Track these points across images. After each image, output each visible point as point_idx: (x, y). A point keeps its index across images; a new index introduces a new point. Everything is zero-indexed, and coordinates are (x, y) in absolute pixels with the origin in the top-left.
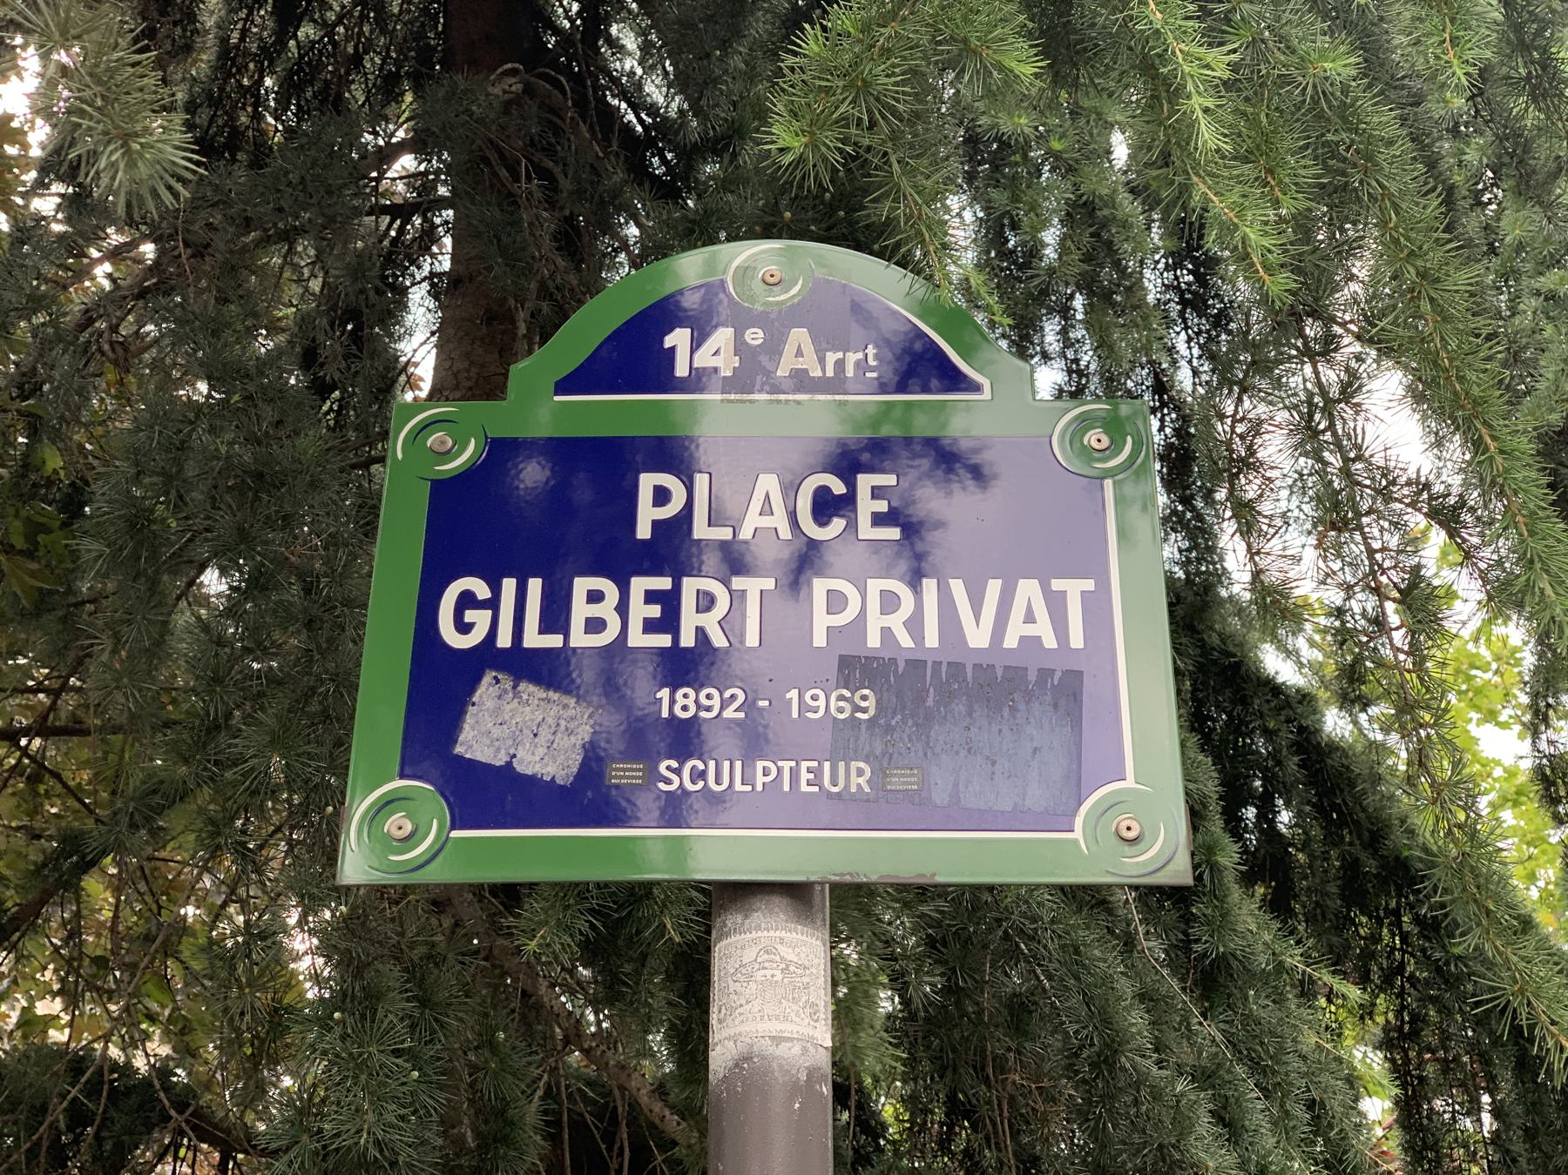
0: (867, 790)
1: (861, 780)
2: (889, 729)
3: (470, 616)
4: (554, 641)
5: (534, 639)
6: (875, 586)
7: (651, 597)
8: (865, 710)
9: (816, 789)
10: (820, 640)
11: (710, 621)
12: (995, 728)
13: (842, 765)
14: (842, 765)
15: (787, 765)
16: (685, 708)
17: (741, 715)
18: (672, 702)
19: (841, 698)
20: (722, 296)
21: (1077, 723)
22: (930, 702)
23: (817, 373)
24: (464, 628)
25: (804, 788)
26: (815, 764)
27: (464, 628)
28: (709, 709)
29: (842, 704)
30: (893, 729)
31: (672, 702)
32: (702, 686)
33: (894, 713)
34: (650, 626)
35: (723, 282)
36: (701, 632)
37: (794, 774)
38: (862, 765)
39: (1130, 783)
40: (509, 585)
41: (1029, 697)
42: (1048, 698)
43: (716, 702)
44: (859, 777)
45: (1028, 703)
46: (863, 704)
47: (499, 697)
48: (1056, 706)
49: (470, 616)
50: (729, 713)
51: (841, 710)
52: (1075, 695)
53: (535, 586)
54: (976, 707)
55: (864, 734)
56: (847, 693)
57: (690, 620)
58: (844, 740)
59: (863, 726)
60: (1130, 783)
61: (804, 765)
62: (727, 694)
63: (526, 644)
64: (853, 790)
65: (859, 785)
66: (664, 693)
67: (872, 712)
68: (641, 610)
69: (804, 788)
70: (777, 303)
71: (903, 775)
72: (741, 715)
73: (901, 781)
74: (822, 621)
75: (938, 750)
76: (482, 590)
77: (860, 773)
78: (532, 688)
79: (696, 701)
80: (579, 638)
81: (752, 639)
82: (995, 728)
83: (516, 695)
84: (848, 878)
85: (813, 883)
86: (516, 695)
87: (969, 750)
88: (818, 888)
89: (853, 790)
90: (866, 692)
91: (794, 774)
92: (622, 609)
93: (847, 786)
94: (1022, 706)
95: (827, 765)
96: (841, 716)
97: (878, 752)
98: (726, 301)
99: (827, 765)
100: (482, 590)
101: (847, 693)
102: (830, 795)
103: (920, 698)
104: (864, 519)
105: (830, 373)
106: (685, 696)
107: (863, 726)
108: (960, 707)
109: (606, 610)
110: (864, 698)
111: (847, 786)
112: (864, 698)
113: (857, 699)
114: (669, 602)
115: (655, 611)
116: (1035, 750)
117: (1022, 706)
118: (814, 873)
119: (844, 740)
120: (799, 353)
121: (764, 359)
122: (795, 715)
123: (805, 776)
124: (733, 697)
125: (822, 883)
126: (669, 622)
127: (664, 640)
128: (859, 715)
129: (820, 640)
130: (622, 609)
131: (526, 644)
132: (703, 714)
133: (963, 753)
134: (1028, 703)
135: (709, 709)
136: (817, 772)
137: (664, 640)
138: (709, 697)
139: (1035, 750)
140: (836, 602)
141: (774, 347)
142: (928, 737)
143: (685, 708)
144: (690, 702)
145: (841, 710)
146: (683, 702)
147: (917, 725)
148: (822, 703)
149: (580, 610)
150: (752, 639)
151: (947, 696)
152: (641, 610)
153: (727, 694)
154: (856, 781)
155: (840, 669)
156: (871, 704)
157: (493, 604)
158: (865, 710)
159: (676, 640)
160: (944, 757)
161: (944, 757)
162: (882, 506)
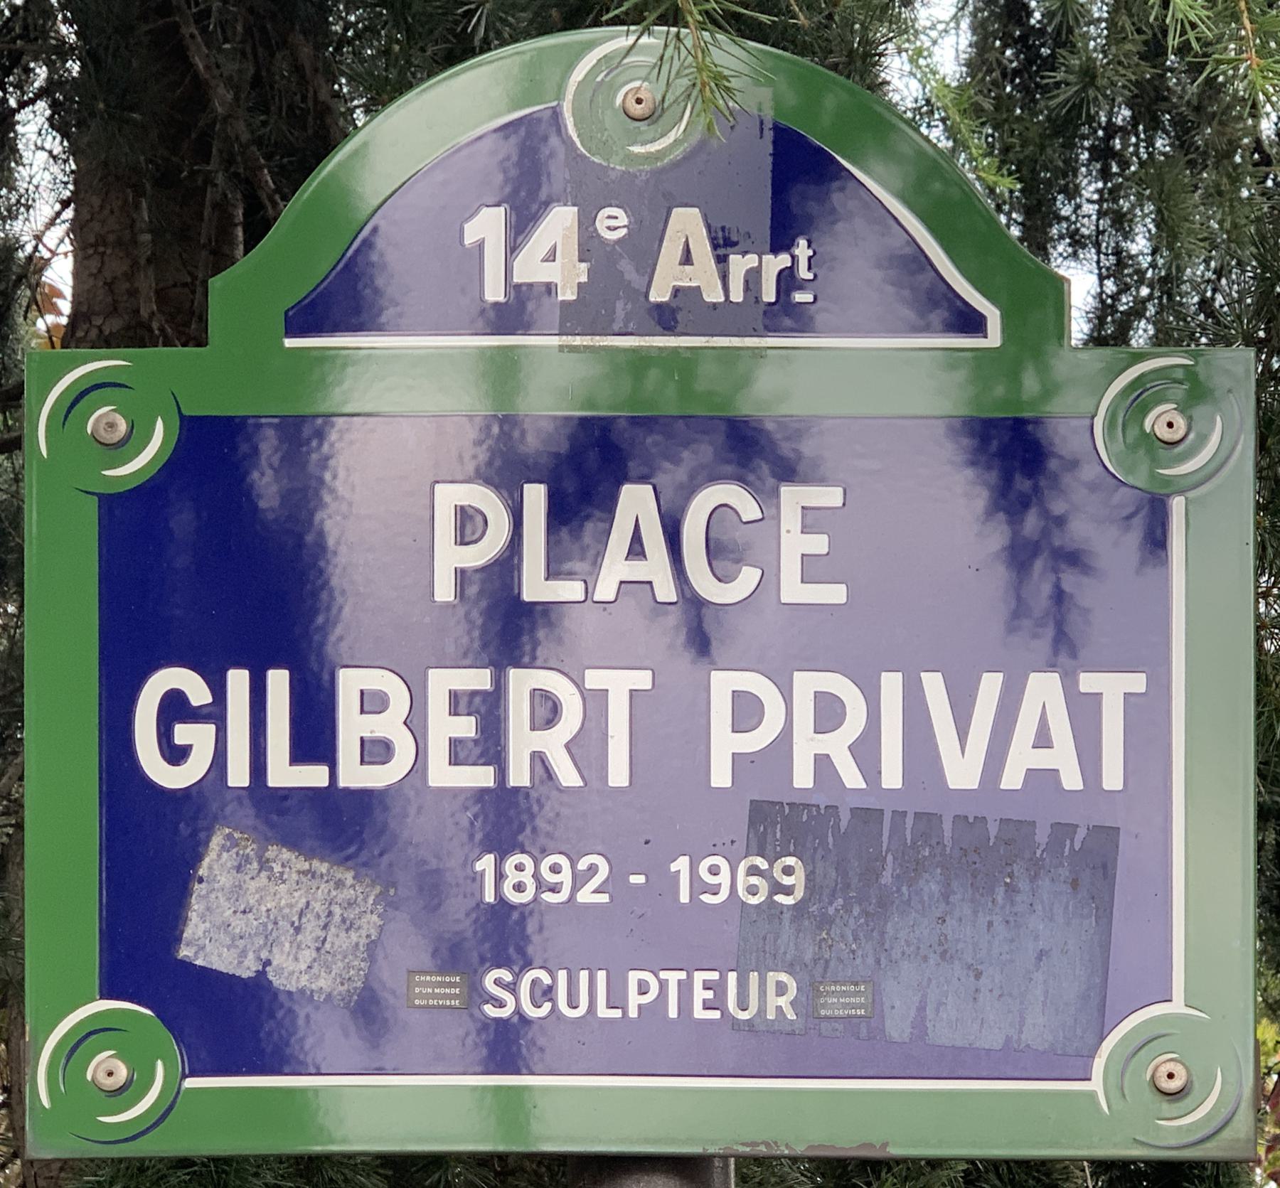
0: (791, 1015)
1: (783, 1001)
2: (825, 921)
3: (183, 733)
4: (314, 776)
5: (284, 773)
6: (807, 684)
7: (457, 703)
8: (788, 891)
9: (716, 1015)
10: (721, 776)
11: (554, 743)
12: (983, 920)
13: (754, 976)
14: (754, 976)
15: (673, 977)
16: (519, 887)
17: (604, 898)
18: (500, 876)
19: (754, 871)
20: (554, 141)
21: (1104, 912)
22: (887, 878)
23: (714, 295)
24: (175, 754)
25: (699, 1013)
26: (714, 976)
27: (175, 754)
28: (554, 889)
29: (754, 880)
30: (831, 921)
31: (500, 876)
32: (545, 852)
33: (833, 896)
34: (458, 753)
35: (556, 114)
36: (539, 760)
37: (685, 989)
38: (784, 977)
39: (1177, 1006)
40: (238, 681)
41: (1036, 869)
42: (1064, 872)
43: (566, 877)
44: (778, 996)
45: (1034, 879)
46: (787, 881)
47: (239, 868)
48: (1075, 884)
49: (183, 733)
50: (586, 896)
51: (753, 891)
52: (1104, 867)
53: (278, 681)
54: (955, 884)
55: (787, 929)
56: (762, 863)
57: (522, 741)
58: (753, 938)
59: (787, 916)
60: (1177, 1006)
61: (699, 977)
62: (583, 865)
63: (272, 782)
64: (771, 1015)
65: (779, 1009)
66: (486, 863)
67: (799, 893)
68: (447, 726)
69: (699, 1013)
70: (648, 157)
71: (845, 994)
72: (604, 898)
73: (841, 1002)
74: (725, 745)
75: (896, 954)
76: (198, 692)
77: (781, 989)
78: (286, 854)
79: (536, 876)
80: (354, 774)
81: (618, 775)
82: (983, 920)
83: (264, 864)
84: (763, 1150)
85: (713, 1156)
86: (264, 864)
87: (943, 955)
88: (717, 1163)
89: (771, 1015)
90: (790, 861)
91: (685, 989)
92: (416, 723)
93: (762, 1010)
94: (1024, 885)
95: (732, 977)
96: (754, 901)
97: (808, 956)
98: (561, 155)
99: (732, 977)
100: (198, 692)
101: (762, 863)
102: (735, 1023)
103: (871, 872)
104: (790, 569)
105: (737, 295)
106: (520, 868)
107: (787, 916)
108: (931, 886)
109: (390, 725)
110: (788, 871)
111: (762, 1010)
112: (788, 871)
113: (777, 873)
114: (489, 709)
115: (466, 727)
116: (1041, 955)
117: (1024, 885)
118: (713, 1142)
119: (753, 938)
120: (687, 259)
121: (627, 267)
122: (684, 897)
123: (700, 995)
124: (593, 869)
125: (725, 1158)
126: (489, 745)
127: (483, 777)
128: (780, 898)
129: (721, 776)
130: (416, 723)
131: (272, 782)
132: (548, 897)
133: (933, 959)
134: (1034, 879)
135: (554, 889)
136: (717, 988)
137: (483, 777)
138: (555, 869)
139: (1041, 955)
140: (746, 712)
141: (644, 244)
142: (882, 933)
143: (519, 887)
144: (527, 877)
145: (753, 891)
146: (515, 878)
147: (867, 914)
148: (724, 878)
149: (351, 727)
150: (618, 775)
151: (912, 869)
152: (447, 726)
153: (583, 865)
154: (774, 1001)
155: (752, 823)
156: (797, 880)
157: (216, 714)
158: (788, 891)
159: (502, 774)
160: (905, 965)
161: (905, 965)
162: (818, 544)
